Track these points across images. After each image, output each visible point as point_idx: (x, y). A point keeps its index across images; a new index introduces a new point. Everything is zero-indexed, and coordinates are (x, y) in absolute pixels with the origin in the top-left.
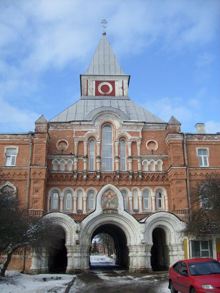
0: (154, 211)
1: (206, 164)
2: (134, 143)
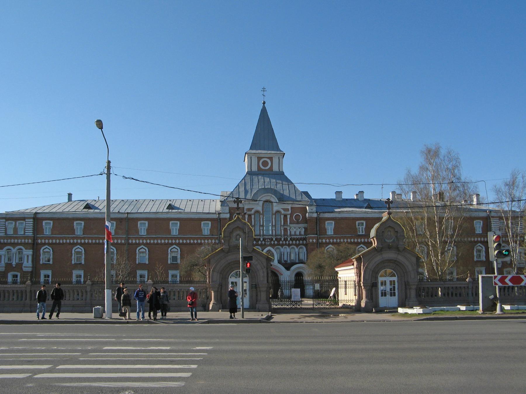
0: (297, 261)
2: (285, 216)
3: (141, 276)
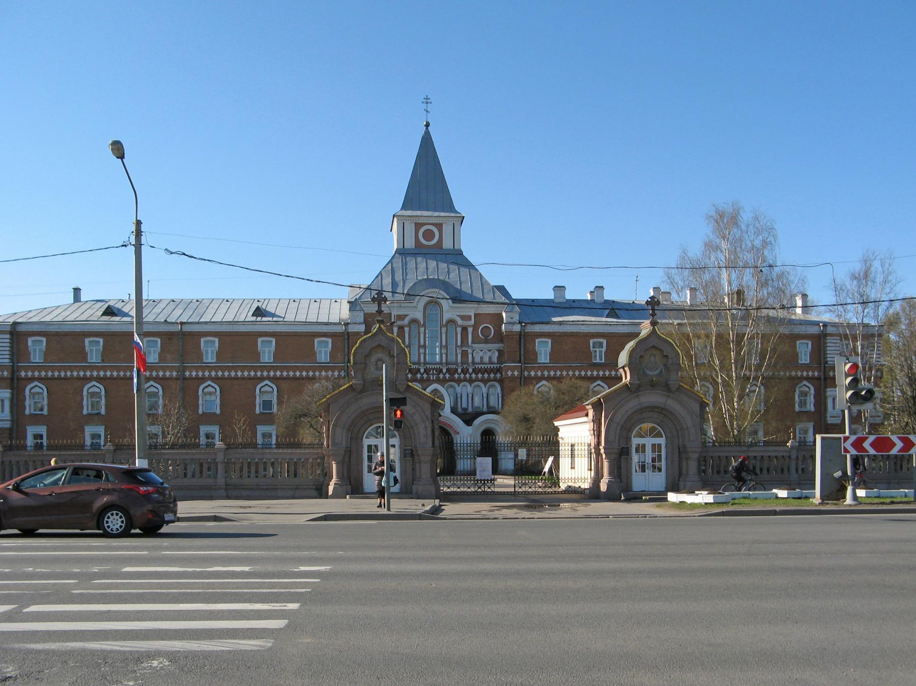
0: (485, 409)
1: (545, 359)
2: (465, 329)
3: (208, 436)
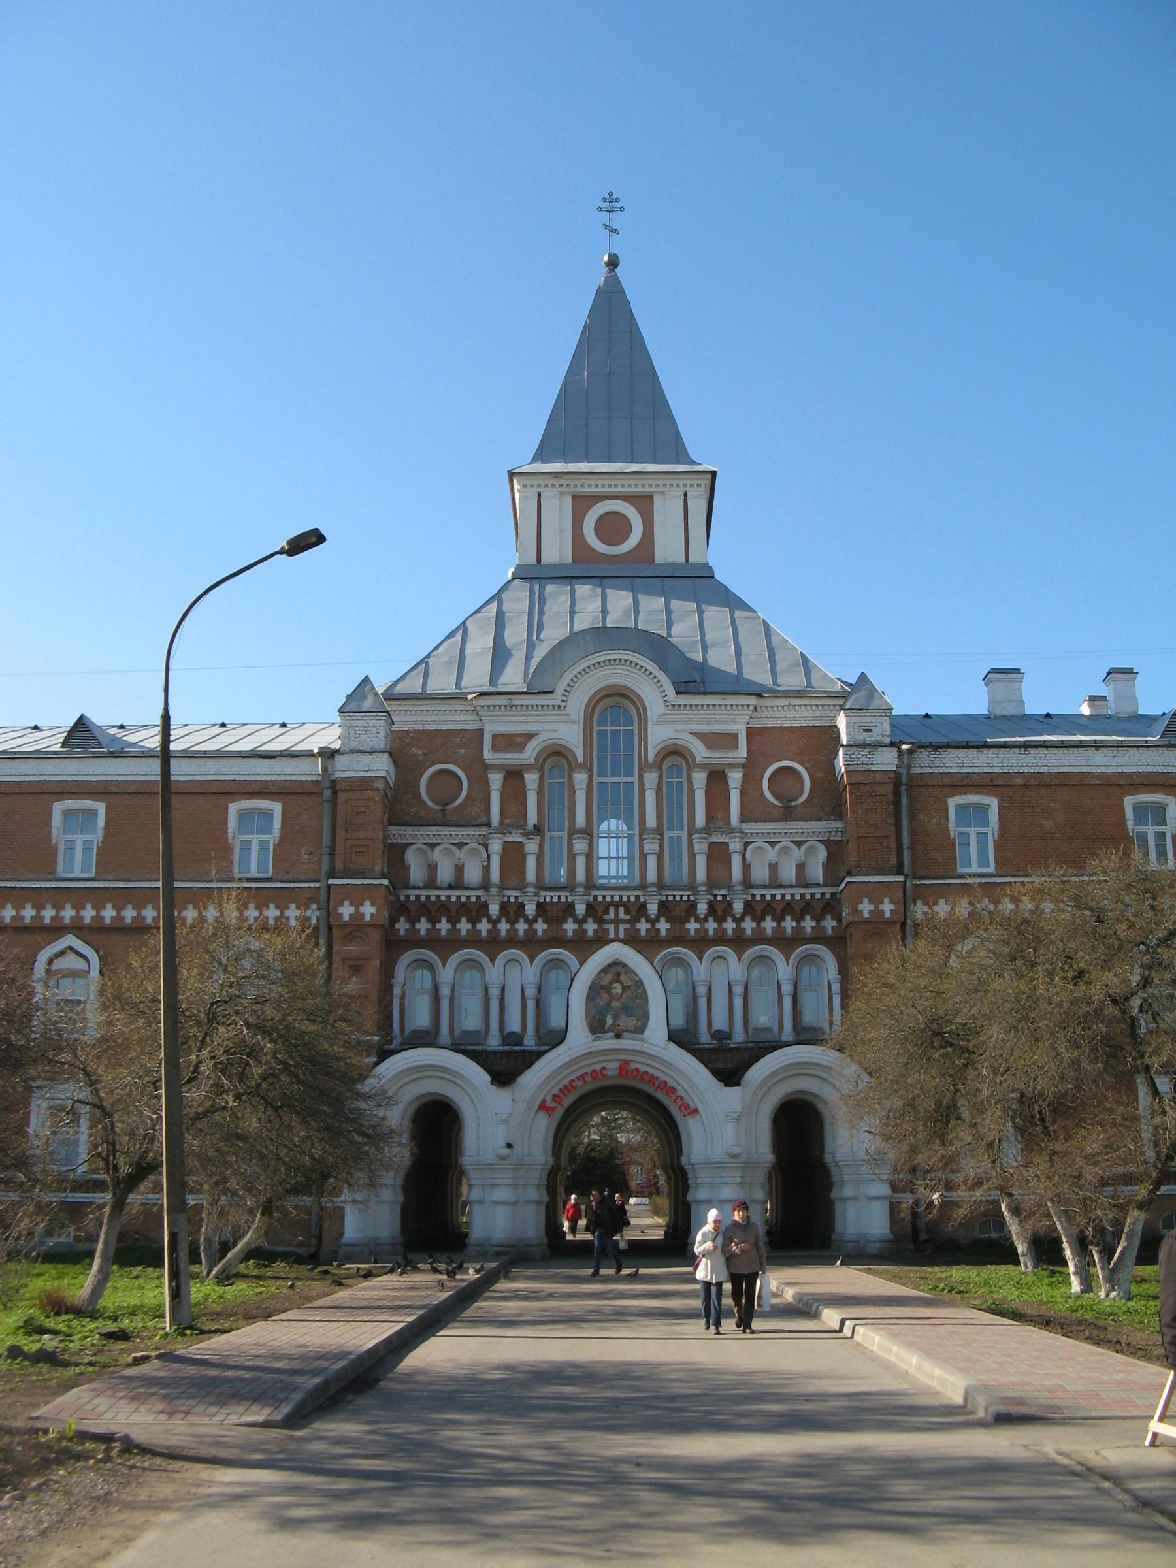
0: (788, 1034)
1: (983, 862)
2: (717, 777)
